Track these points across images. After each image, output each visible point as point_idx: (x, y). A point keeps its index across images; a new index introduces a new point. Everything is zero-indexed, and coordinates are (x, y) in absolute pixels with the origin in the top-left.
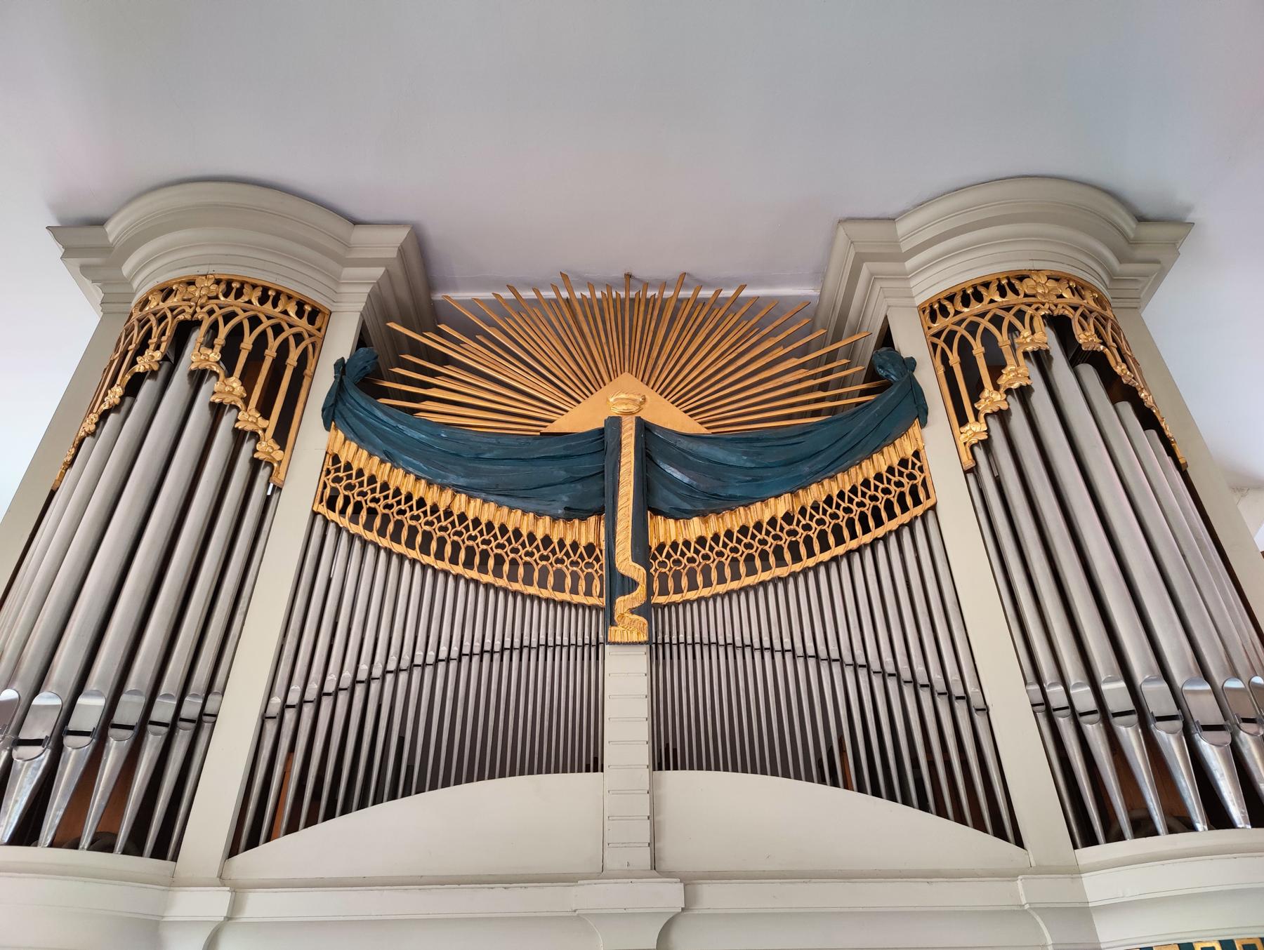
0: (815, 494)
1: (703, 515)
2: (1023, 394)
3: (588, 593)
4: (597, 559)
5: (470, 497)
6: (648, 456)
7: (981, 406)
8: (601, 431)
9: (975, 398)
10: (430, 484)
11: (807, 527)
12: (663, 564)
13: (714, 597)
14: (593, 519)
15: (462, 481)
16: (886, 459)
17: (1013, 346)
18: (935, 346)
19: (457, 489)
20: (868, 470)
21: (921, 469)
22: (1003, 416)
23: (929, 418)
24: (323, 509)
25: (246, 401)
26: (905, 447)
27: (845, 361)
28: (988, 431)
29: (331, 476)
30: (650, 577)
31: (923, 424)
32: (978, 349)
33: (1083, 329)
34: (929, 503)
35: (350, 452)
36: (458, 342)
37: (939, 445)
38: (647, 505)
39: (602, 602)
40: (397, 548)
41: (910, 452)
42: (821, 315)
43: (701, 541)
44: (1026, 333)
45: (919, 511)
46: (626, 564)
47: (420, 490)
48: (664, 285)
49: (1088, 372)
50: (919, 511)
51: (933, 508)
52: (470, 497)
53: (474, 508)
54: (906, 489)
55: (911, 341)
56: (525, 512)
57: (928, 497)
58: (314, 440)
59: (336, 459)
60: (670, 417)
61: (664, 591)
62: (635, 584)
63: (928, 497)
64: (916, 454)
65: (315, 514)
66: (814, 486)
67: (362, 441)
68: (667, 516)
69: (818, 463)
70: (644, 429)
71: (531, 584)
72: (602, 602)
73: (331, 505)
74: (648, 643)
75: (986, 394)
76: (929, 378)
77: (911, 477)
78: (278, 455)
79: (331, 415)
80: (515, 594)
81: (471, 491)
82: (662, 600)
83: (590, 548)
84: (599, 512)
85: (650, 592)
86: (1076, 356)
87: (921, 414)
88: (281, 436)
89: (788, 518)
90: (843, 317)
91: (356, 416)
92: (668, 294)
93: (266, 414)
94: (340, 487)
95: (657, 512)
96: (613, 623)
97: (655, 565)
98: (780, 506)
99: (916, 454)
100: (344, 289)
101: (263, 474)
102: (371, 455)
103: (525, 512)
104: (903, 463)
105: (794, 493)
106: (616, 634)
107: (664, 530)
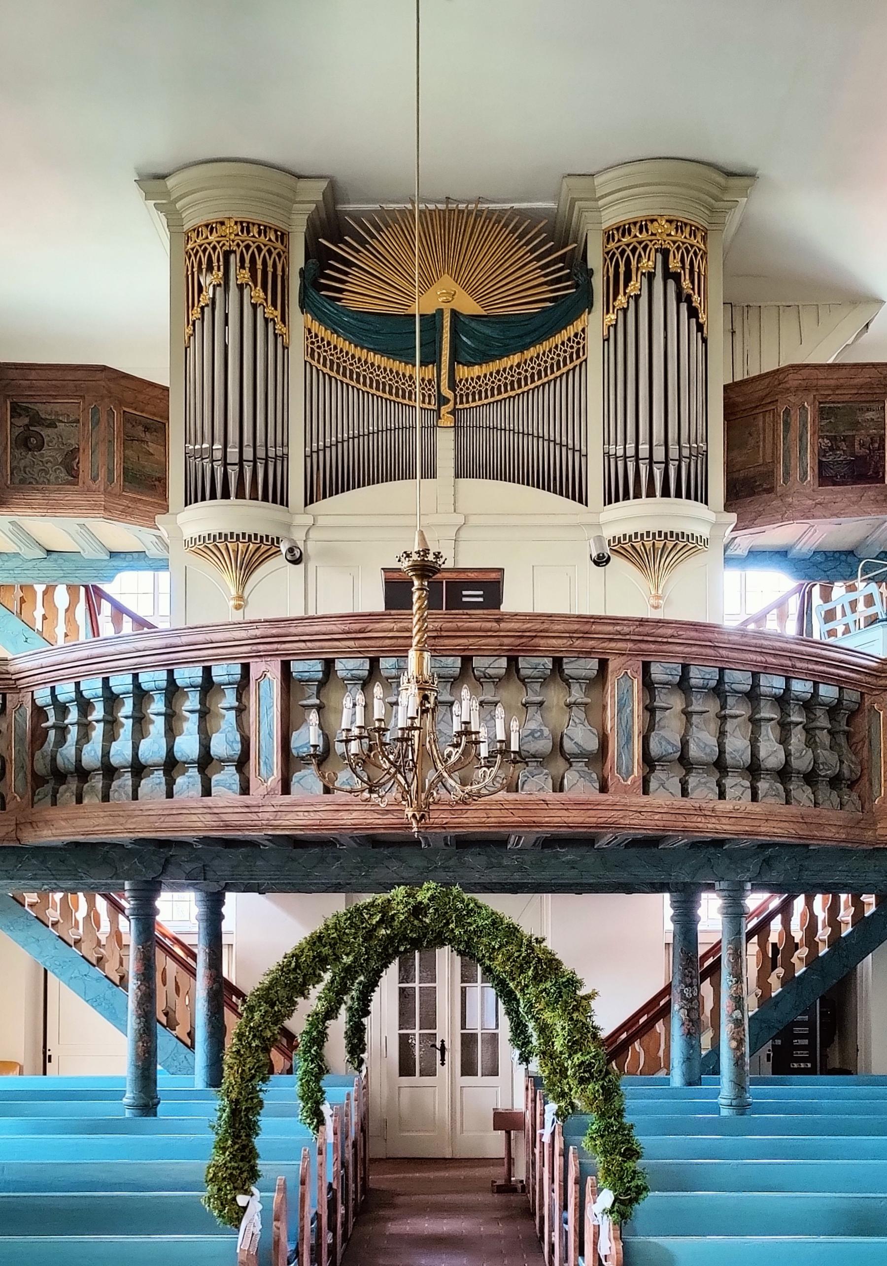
0: (532, 352)
1: (480, 364)
2: (637, 297)
3: (429, 403)
4: (433, 387)
5: (375, 354)
6: (455, 331)
7: (617, 303)
8: (434, 315)
9: (615, 299)
10: (356, 346)
11: (526, 371)
12: (461, 389)
13: (483, 405)
14: (431, 366)
15: (372, 347)
16: (571, 331)
17: (638, 269)
18: (605, 260)
19: (369, 350)
20: (558, 339)
21: (584, 339)
22: (625, 311)
23: (593, 308)
24: (309, 360)
25: (266, 300)
26: (578, 325)
27: (561, 265)
28: (617, 320)
29: (309, 341)
30: (455, 396)
31: (589, 313)
32: (622, 269)
33: (675, 258)
34: (585, 357)
35: (316, 327)
36: (358, 251)
37: (594, 324)
38: (455, 358)
39: (435, 408)
40: (345, 380)
41: (580, 329)
42: (558, 226)
43: (479, 378)
44: (645, 261)
45: (579, 361)
46: (446, 392)
47: (352, 349)
48: (469, 202)
49: (671, 284)
50: (579, 361)
51: (586, 360)
52: (375, 354)
53: (378, 359)
54: (574, 350)
55: (595, 260)
56: (400, 362)
57: (584, 354)
58: (299, 322)
59: (310, 331)
60: (469, 306)
61: (461, 403)
62: (449, 400)
63: (584, 354)
64: (583, 330)
65: (306, 362)
66: (532, 349)
67: (321, 322)
68: (464, 365)
69: (535, 335)
70: (454, 314)
71: (405, 398)
72: (435, 408)
73: (313, 358)
74: (455, 427)
75: (620, 297)
76: (598, 283)
77: (578, 343)
78: (284, 330)
79: (303, 306)
80: (398, 403)
81: (376, 351)
82: (461, 407)
83: (430, 381)
84: (433, 363)
85: (455, 403)
86: (668, 274)
87: (590, 305)
88: (283, 320)
89: (518, 366)
90: (568, 231)
91: (315, 306)
92: (472, 206)
93: (276, 309)
94: (315, 347)
95: (459, 363)
96: (440, 418)
97: (458, 390)
98: (516, 359)
99: (583, 330)
100: (293, 217)
101: (280, 339)
102: (326, 329)
103: (400, 362)
104: (576, 335)
105: (522, 352)
106: (441, 423)
107: (463, 372)
